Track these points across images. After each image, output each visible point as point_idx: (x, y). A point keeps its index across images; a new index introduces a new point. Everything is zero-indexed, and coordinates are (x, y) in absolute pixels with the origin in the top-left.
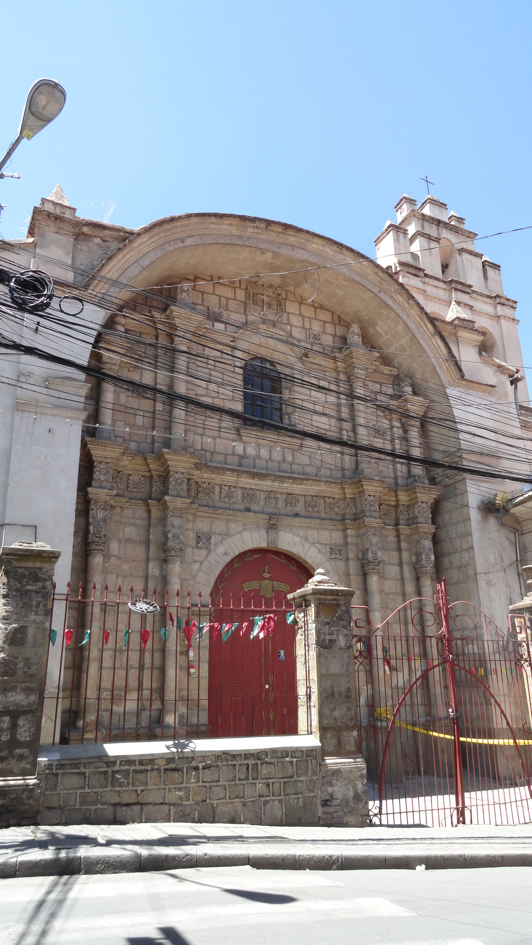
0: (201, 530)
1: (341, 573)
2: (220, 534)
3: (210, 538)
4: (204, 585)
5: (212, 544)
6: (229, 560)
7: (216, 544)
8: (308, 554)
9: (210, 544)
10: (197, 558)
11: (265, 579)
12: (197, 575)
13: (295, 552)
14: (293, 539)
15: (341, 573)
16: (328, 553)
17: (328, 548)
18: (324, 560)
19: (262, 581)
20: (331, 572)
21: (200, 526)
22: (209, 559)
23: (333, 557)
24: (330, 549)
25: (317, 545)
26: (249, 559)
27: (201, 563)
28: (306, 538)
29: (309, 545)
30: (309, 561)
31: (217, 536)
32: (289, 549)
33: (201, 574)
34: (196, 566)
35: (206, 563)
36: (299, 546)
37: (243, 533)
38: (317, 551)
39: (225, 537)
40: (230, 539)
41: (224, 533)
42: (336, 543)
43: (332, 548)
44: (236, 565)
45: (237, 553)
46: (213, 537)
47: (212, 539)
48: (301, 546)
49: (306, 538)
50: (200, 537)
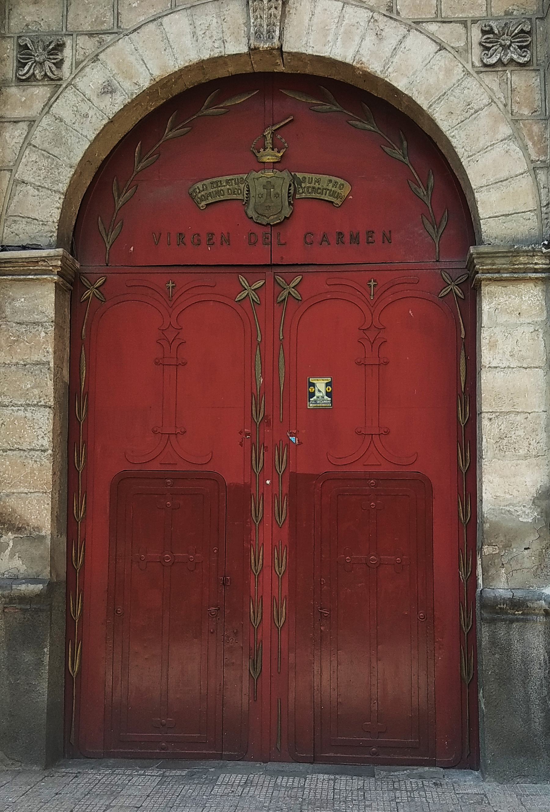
0: (33, 27)
1: (526, 112)
2: (91, 35)
3: (60, 47)
4: (38, 188)
5: (66, 66)
6: (117, 108)
7: (78, 64)
8: (396, 59)
9: (59, 64)
10: (18, 113)
11: (264, 166)
12: (17, 162)
13: (349, 60)
14: (341, 18)
15: (526, 112)
16: (477, 51)
17: (476, 34)
18: (458, 71)
19: (254, 174)
20: (483, 113)
21: (28, 19)
22: (54, 110)
23: (494, 60)
24: (484, 32)
25: (433, 28)
26: (211, 111)
27: (32, 122)
28: (390, 9)
29: (403, 30)
30: (401, 84)
31: (82, 41)
32: (325, 52)
33: (30, 156)
34: (17, 133)
35: (45, 121)
36: (363, 39)
37: (165, 20)
38: (434, 47)
39: (108, 38)
40: (124, 45)
41: (105, 27)
42: (507, 13)
43: (491, 31)
44: (170, 135)
45: (146, 84)
46: (69, 42)
47: (67, 52)
48: (370, 38)
49: (390, 9)
50: (26, 47)
